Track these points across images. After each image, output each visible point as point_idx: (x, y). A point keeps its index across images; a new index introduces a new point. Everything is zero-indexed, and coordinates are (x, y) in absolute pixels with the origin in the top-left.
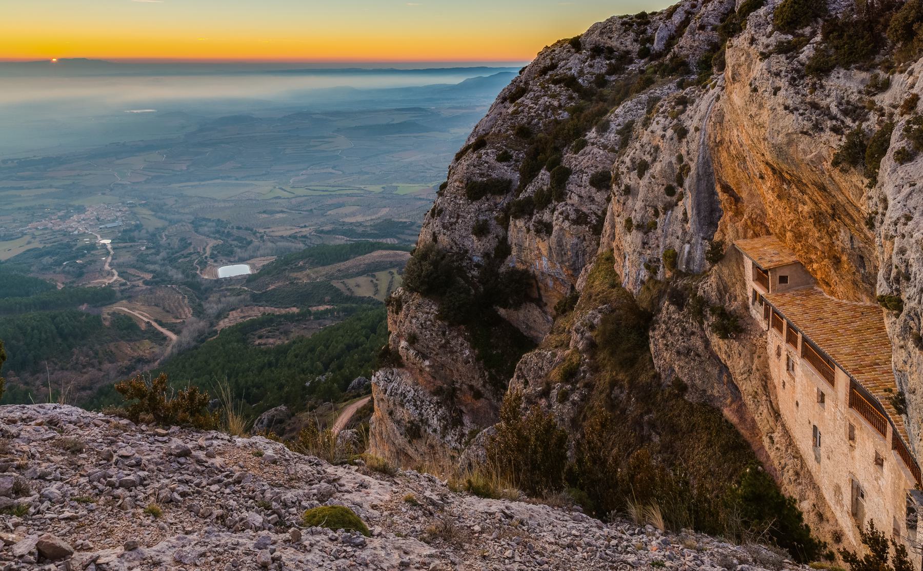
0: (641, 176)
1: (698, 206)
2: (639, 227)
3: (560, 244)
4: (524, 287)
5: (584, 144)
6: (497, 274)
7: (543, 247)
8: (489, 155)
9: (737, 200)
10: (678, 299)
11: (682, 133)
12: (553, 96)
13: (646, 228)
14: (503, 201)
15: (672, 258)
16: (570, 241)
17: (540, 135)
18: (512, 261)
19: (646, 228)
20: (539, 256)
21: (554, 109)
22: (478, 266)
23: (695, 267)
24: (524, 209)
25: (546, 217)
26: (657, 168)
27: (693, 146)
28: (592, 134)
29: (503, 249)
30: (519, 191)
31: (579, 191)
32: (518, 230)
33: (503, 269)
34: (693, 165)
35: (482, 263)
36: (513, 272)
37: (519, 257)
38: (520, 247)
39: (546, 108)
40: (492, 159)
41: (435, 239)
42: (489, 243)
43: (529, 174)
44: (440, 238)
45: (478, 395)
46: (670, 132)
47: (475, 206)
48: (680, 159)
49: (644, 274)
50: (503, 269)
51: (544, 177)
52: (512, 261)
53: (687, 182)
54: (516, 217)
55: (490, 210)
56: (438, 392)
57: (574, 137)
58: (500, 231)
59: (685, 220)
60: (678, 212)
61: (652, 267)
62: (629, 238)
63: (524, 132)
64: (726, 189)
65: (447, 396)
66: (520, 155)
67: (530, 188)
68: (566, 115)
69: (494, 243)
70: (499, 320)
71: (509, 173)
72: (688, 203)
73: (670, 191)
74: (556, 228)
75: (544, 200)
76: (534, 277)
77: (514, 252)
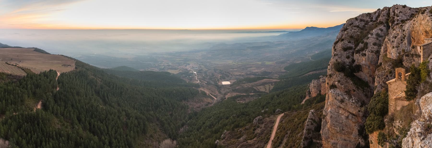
0: (395, 38)
1: (408, 41)
2: (396, 47)
3: (368, 57)
4: (359, 68)
5: (368, 38)
6: (352, 66)
7: (364, 59)
8: (346, 42)
9: (414, 39)
10: (407, 56)
11: (404, 30)
12: (355, 30)
13: (397, 47)
14: (351, 51)
15: (404, 51)
16: (371, 56)
17: (355, 37)
18: (356, 63)
19: (397, 47)
20: (362, 61)
21: (356, 32)
22: (348, 65)
23: (408, 51)
24: (358, 52)
25: (364, 52)
26: (399, 36)
27: (407, 33)
28: (369, 36)
29: (353, 61)
30: (355, 49)
31: (371, 47)
32: (356, 56)
33: (354, 65)
34: (407, 35)
35: (349, 64)
36: (357, 65)
37: (357, 62)
38: (358, 60)
39: (354, 32)
40: (347, 42)
41: (337, 60)
42: (350, 60)
43: (357, 45)
44: (338, 60)
45: (354, 91)
46: (400, 31)
47: (346, 52)
48: (404, 35)
49: (398, 55)
50: (354, 65)
51: (361, 45)
52: (356, 63)
53: (406, 38)
54: (356, 53)
55: (349, 53)
56: (346, 92)
57: (366, 36)
58: (352, 57)
59: (405, 44)
60: (404, 43)
61: (399, 53)
62: (394, 49)
63: (351, 37)
64: (413, 38)
65: (348, 93)
66: (352, 41)
67: (358, 48)
68: (359, 33)
69: (351, 60)
70: (355, 76)
71: (350, 45)
72: (406, 41)
73: (402, 40)
74: (367, 54)
75: (362, 49)
76: (361, 66)
77: (356, 61)
